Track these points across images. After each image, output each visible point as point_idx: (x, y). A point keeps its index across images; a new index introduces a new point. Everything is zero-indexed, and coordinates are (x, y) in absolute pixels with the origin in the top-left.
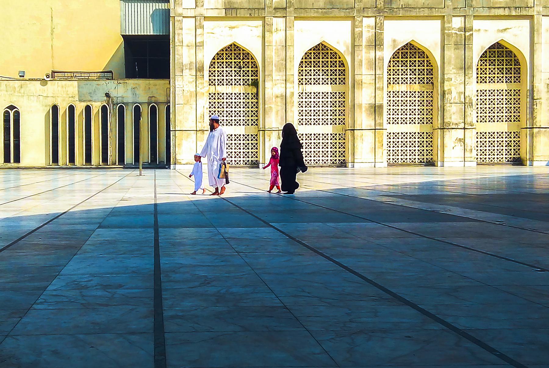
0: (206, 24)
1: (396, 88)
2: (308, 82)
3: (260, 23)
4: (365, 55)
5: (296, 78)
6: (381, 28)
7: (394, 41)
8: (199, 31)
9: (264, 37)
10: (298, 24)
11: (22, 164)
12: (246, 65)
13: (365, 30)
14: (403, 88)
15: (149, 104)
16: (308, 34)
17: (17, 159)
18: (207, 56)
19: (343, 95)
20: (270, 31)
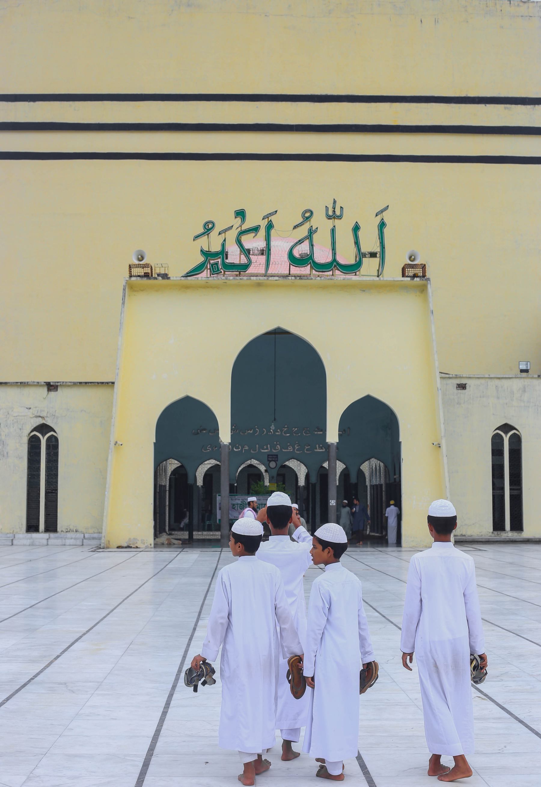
11: (528, 532)
17: (517, 524)
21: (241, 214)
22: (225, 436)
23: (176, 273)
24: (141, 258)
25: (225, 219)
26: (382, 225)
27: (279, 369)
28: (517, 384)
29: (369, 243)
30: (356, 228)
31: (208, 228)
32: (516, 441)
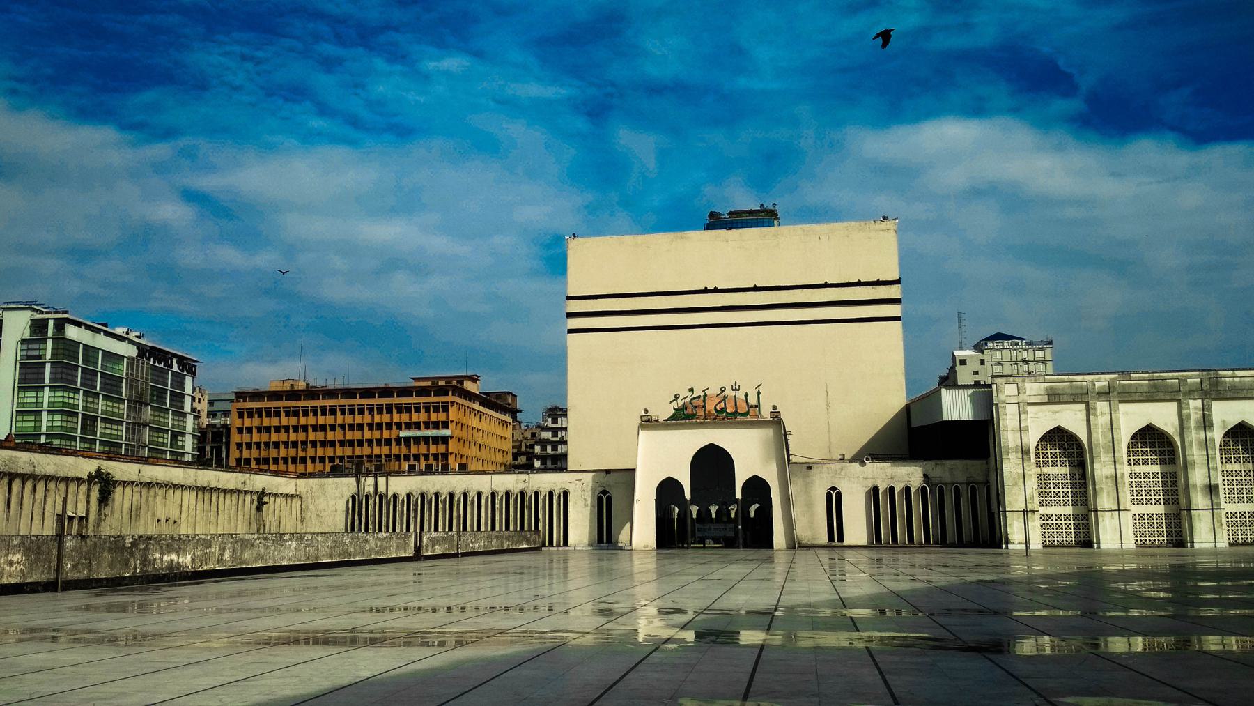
0: (1029, 408)
1: (1230, 467)
2: (1137, 463)
3: (1083, 406)
4: (1194, 436)
5: (1125, 458)
6: (1210, 409)
7: (1224, 422)
8: (1023, 416)
9: (1088, 420)
10: (1122, 407)
12: (1071, 446)
13: (1191, 411)
14: (1237, 467)
15: (968, 484)
16: (1132, 417)
17: (841, 538)
18: (1032, 439)
19: (1174, 475)
20: (1095, 415)
21: (691, 390)
22: (688, 495)
23: (661, 421)
24: (646, 411)
25: (684, 393)
26: (759, 393)
27: (711, 464)
28: (838, 466)
29: (753, 400)
30: (746, 395)
31: (677, 397)
32: (839, 496)
